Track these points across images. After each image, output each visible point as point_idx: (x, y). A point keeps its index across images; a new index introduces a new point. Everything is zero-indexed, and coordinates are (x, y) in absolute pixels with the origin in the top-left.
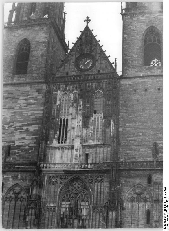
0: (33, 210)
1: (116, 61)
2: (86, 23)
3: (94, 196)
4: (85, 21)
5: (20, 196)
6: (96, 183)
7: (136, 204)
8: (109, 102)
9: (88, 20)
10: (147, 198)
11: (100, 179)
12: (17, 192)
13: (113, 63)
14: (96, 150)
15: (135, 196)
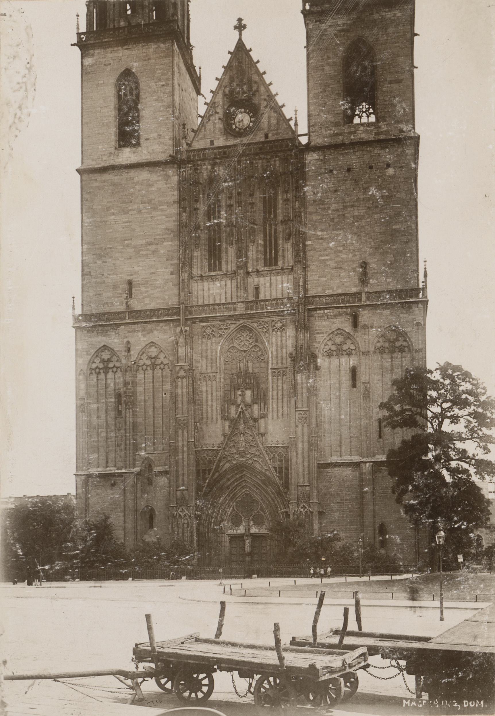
0: (184, 380)
1: (296, 114)
2: (237, 33)
3: (272, 352)
4: (236, 27)
5: (158, 362)
6: (274, 333)
7: (335, 361)
8: (287, 197)
9: (240, 27)
10: (352, 350)
11: (279, 325)
12: (153, 356)
13: (291, 119)
14: (271, 279)
15: (334, 348)
